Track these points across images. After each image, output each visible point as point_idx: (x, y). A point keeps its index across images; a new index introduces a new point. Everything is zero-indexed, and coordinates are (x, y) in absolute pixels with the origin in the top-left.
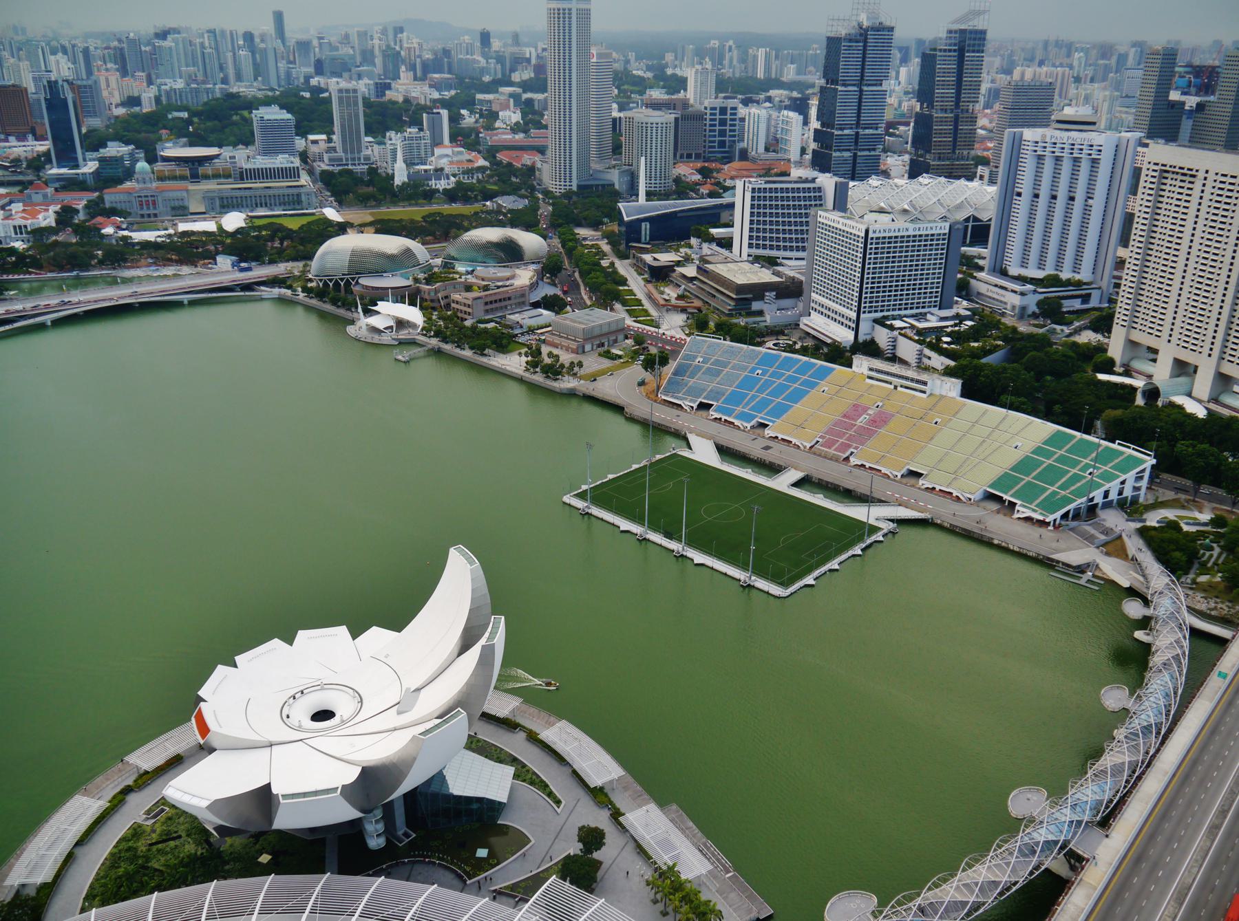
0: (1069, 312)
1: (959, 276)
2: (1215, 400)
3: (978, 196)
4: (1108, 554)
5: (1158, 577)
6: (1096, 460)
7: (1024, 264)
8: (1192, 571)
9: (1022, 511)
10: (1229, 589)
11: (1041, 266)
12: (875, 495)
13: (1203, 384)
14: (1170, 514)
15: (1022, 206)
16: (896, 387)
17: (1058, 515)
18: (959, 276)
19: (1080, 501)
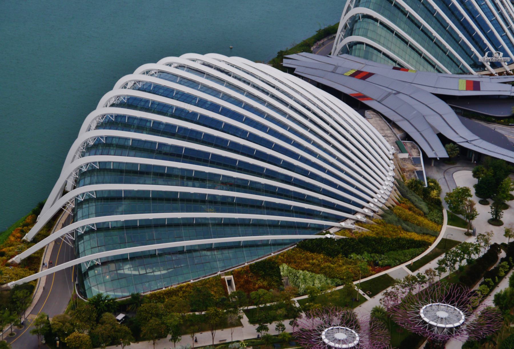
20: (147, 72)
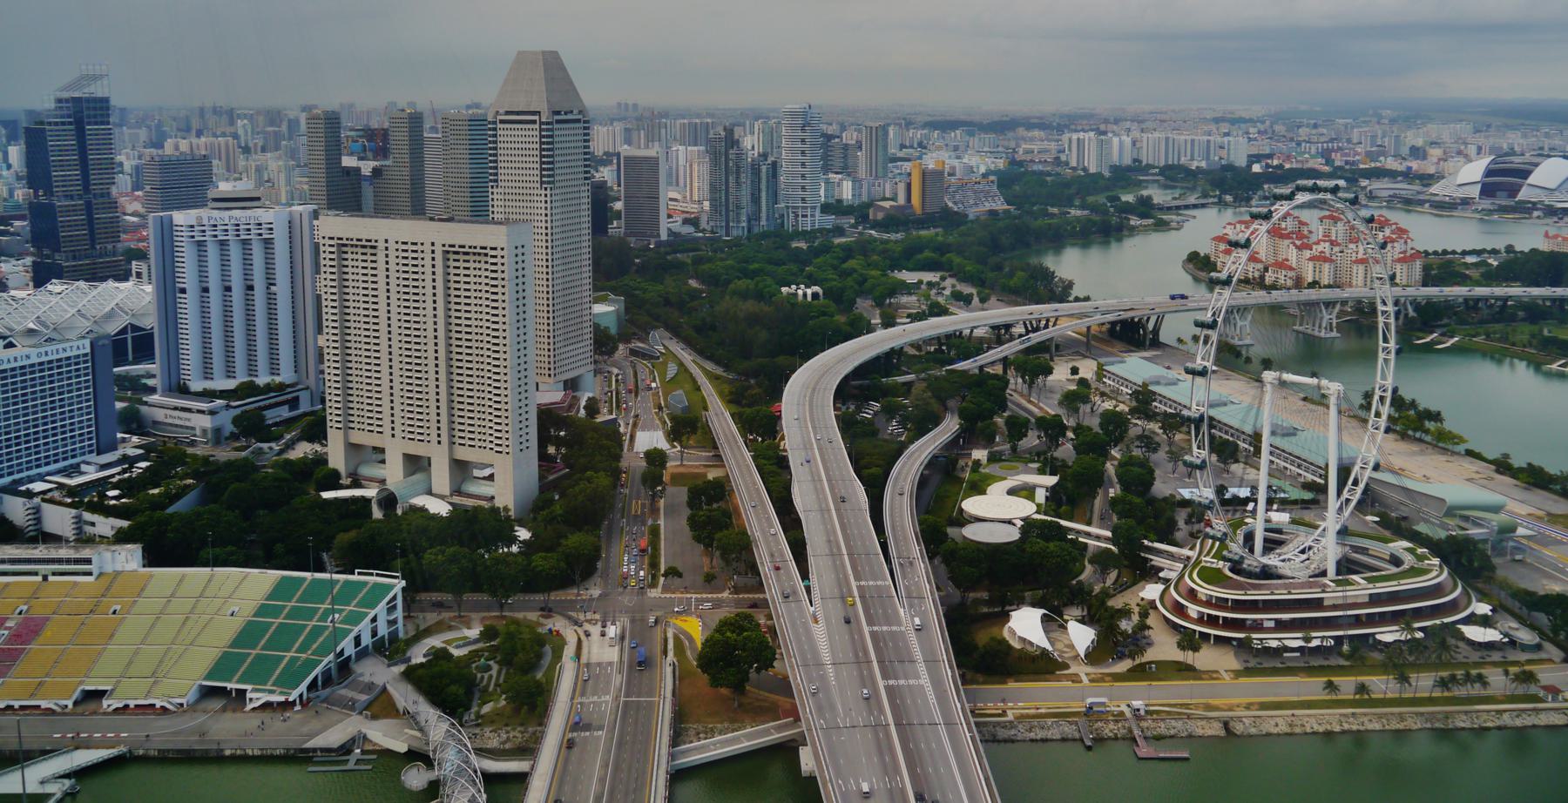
0: (276, 424)
1: (119, 405)
2: (457, 491)
3: (130, 299)
4: (374, 717)
5: (437, 725)
6: (332, 603)
7: (207, 376)
8: (476, 702)
9: (257, 698)
10: (517, 711)
11: (230, 374)
12: (35, 747)
13: (441, 477)
14: (436, 642)
15: (189, 305)
16: (45, 578)
17: (303, 687)
18: (119, 405)
19: (326, 660)
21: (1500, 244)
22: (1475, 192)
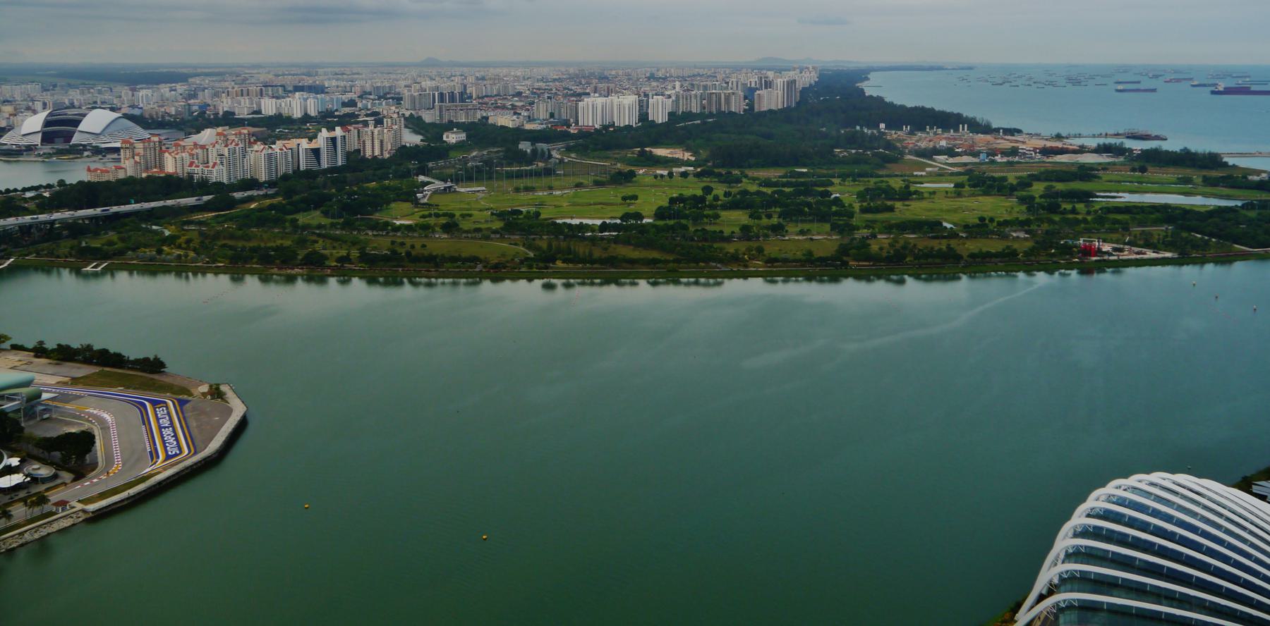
20: (1118, 487)
21: (53, 180)
22: (37, 140)
